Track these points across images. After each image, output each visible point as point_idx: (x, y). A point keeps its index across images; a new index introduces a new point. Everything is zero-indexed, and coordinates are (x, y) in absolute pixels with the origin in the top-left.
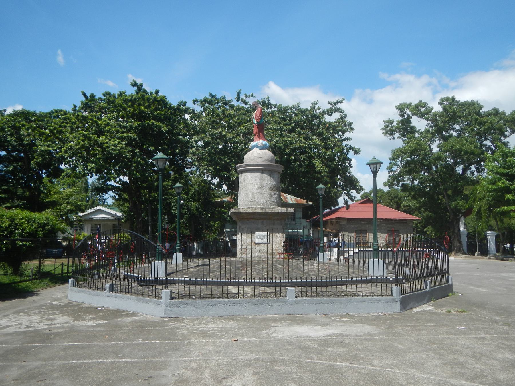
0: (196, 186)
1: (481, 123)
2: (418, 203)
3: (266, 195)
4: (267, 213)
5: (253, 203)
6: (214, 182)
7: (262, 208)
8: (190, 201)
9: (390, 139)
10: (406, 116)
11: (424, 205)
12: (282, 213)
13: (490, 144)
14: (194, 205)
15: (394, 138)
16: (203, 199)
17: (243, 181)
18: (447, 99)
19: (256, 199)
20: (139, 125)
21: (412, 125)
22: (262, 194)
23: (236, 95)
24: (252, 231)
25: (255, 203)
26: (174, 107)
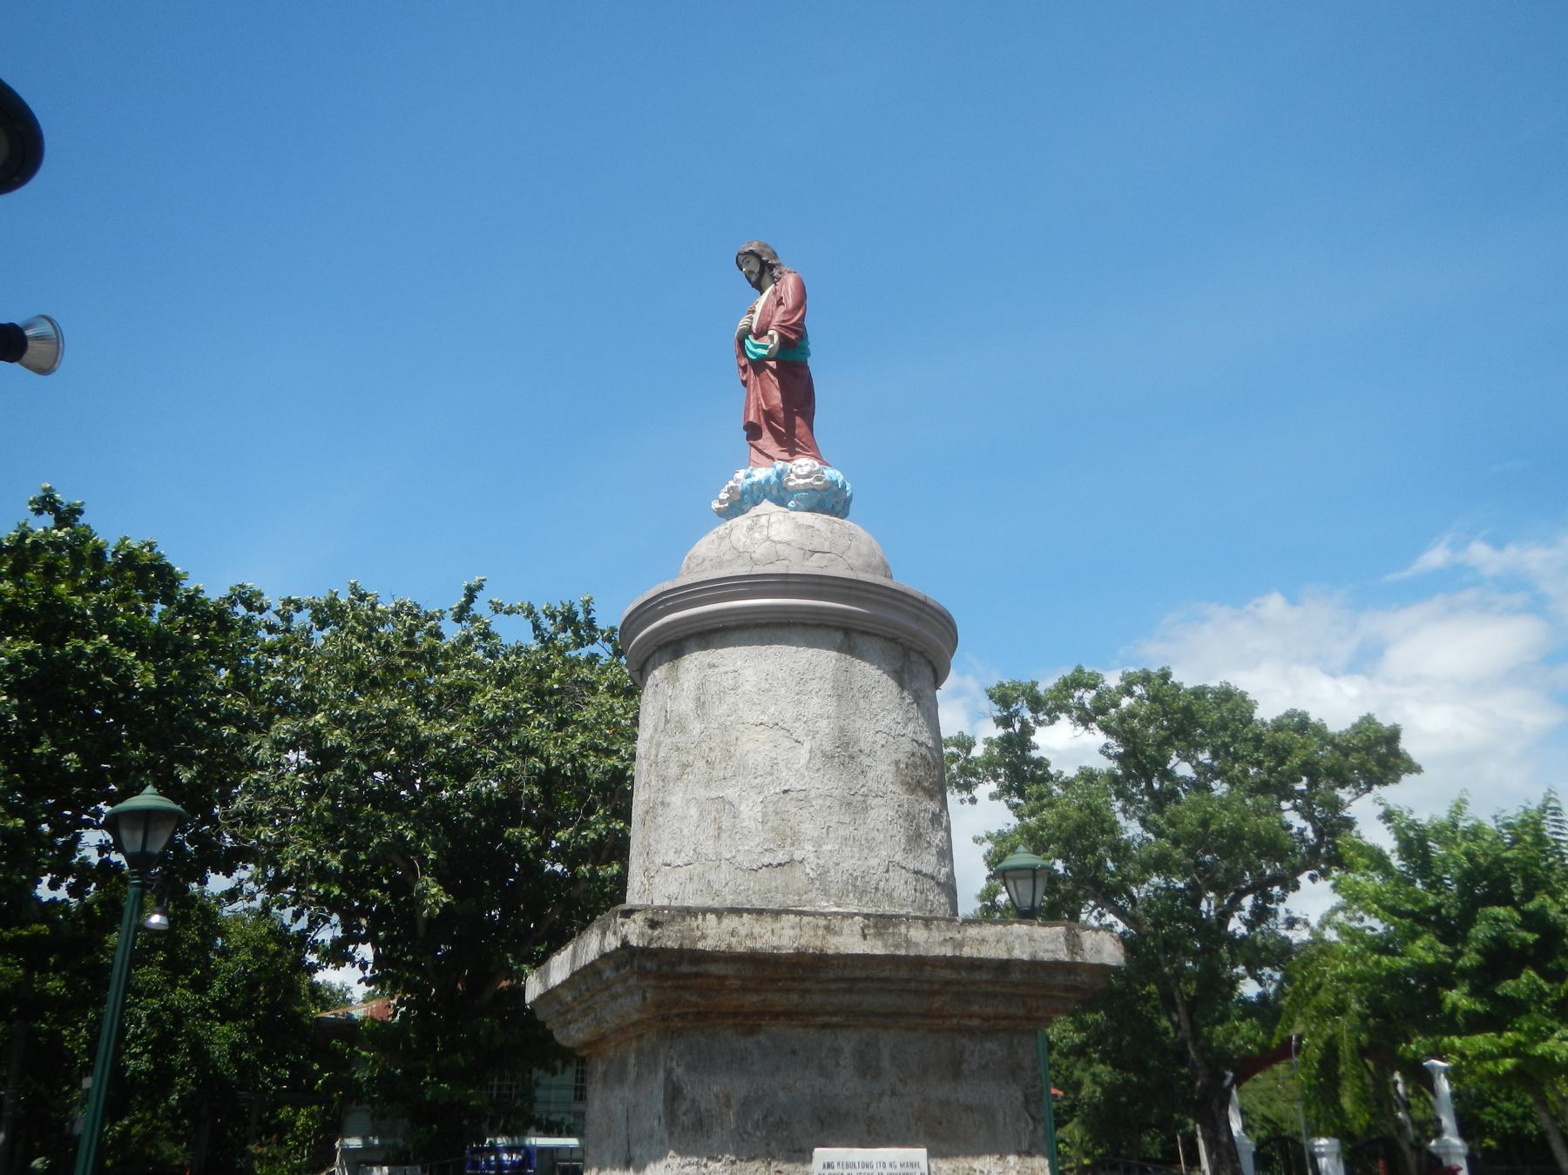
0: (244, 956)
1: (1280, 753)
2: (1077, 1030)
4: (920, 962)
5: (779, 878)
6: (319, 937)
7: (881, 923)
9: (962, 801)
10: (1017, 726)
11: (1098, 1037)
12: (1034, 966)
13: (1303, 824)
14: (226, 1036)
16: (266, 1007)
17: (685, 705)
18: (1146, 678)
19: (806, 851)
20: (30, 656)
21: (1035, 754)
22: (856, 805)
25: (798, 876)
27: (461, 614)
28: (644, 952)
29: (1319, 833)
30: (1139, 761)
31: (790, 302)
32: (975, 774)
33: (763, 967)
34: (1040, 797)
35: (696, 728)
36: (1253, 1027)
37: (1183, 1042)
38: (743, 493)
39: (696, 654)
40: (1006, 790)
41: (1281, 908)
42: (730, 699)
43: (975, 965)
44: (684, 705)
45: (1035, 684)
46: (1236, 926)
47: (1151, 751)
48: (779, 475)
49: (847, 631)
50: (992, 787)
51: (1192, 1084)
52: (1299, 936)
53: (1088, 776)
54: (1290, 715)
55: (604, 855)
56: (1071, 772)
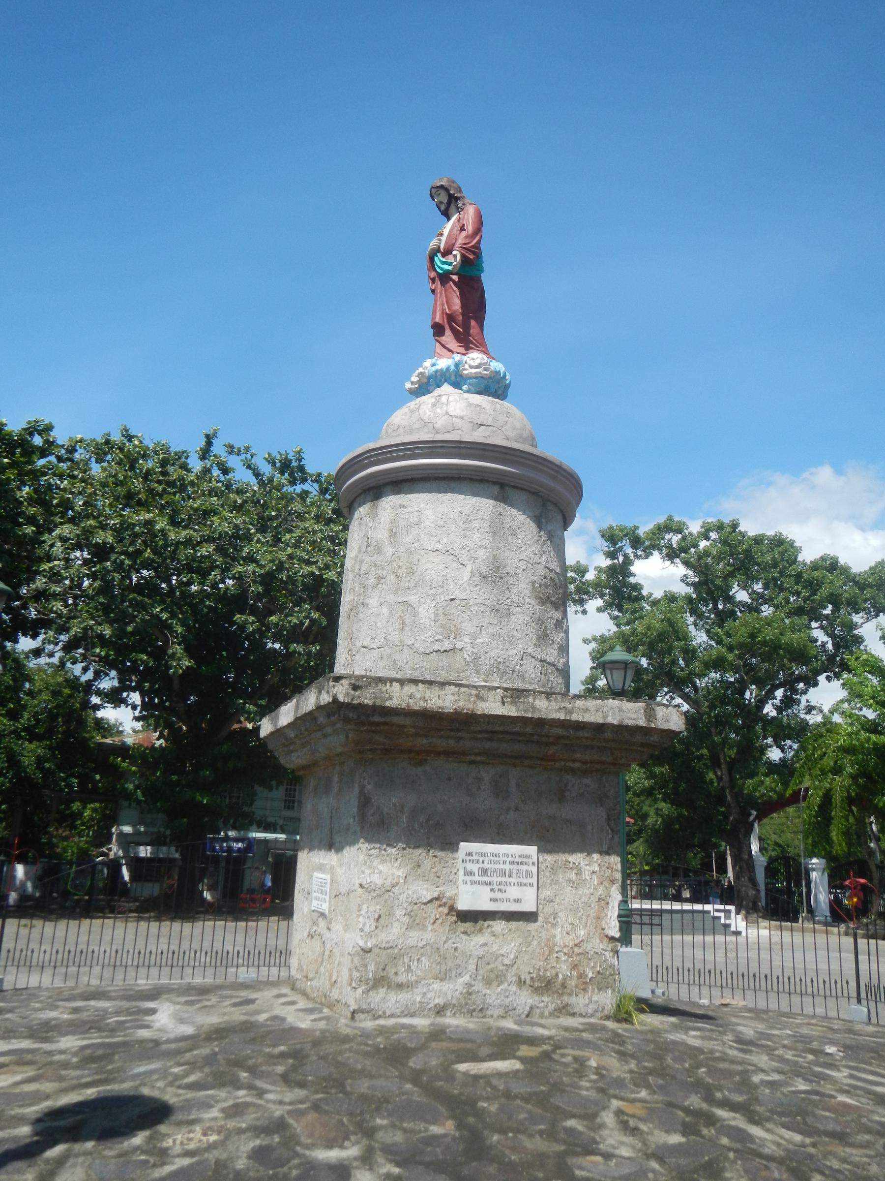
0: (45, 696)
1: (813, 586)
3: (520, 619)
4: (541, 723)
5: (445, 660)
6: (101, 686)
7: (516, 694)
8: (19, 737)
9: (576, 612)
10: (621, 559)
11: (661, 783)
12: (621, 729)
15: (584, 612)
17: (381, 535)
18: (720, 527)
19: (464, 642)
21: (632, 580)
22: (501, 612)
23: (203, 442)
24: (439, 833)
25: (458, 660)
26: (10, 434)
27: (205, 454)
28: (348, 706)
29: (836, 646)
30: (709, 588)
31: (470, 228)
32: (587, 593)
33: (431, 720)
34: (634, 612)
35: (389, 551)
36: (774, 781)
37: (723, 789)
38: (429, 378)
39: (391, 497)
40: (609, 605)
41: (803, 699)
42: (415, 531)
43: (580, 726)
44: (381, 535)
45: (636, 528)
46: (769, 710)
47: (718, 582)
48: (457, 365)
49: (502, 485)
50: (599, 602)
51: (726, 818)
52: (814, 719)
53: (671, 598)
54: (823, 559)
55: (311, 638)
56: (658, 594)
